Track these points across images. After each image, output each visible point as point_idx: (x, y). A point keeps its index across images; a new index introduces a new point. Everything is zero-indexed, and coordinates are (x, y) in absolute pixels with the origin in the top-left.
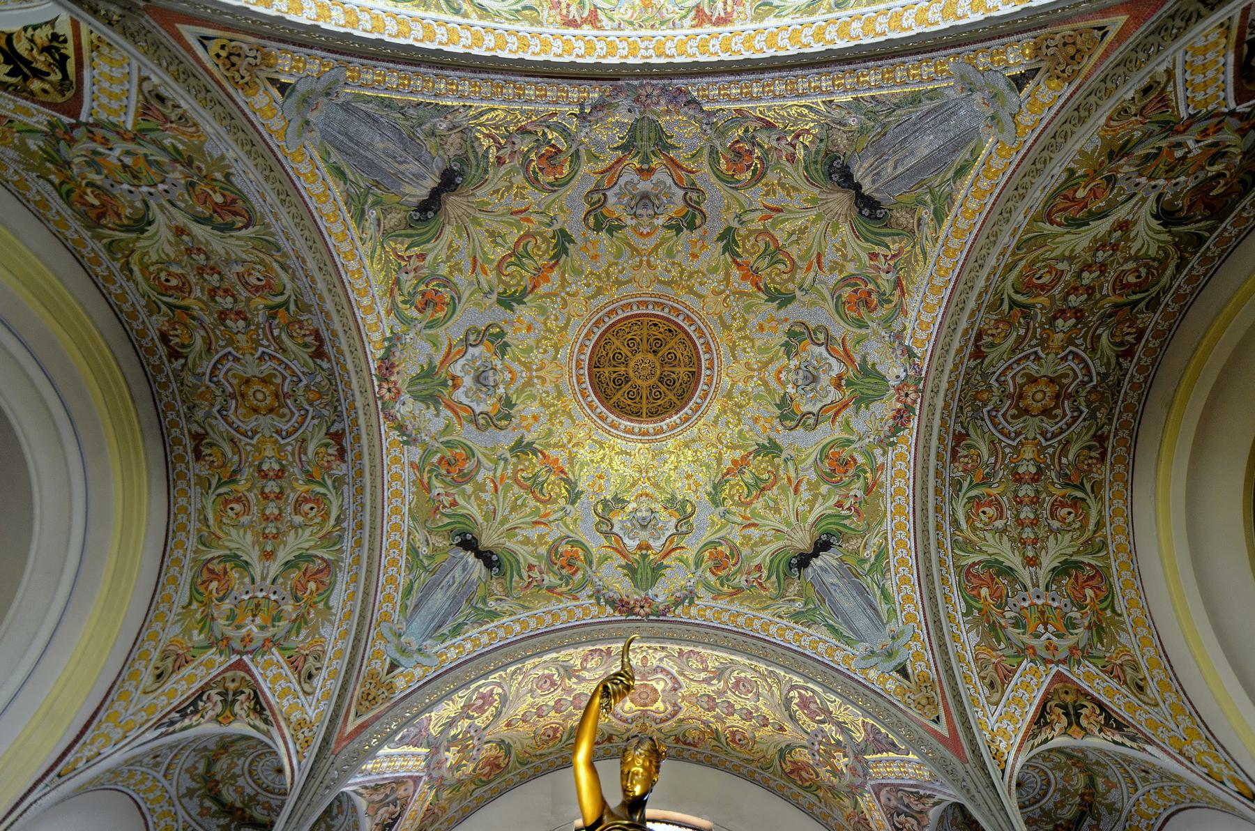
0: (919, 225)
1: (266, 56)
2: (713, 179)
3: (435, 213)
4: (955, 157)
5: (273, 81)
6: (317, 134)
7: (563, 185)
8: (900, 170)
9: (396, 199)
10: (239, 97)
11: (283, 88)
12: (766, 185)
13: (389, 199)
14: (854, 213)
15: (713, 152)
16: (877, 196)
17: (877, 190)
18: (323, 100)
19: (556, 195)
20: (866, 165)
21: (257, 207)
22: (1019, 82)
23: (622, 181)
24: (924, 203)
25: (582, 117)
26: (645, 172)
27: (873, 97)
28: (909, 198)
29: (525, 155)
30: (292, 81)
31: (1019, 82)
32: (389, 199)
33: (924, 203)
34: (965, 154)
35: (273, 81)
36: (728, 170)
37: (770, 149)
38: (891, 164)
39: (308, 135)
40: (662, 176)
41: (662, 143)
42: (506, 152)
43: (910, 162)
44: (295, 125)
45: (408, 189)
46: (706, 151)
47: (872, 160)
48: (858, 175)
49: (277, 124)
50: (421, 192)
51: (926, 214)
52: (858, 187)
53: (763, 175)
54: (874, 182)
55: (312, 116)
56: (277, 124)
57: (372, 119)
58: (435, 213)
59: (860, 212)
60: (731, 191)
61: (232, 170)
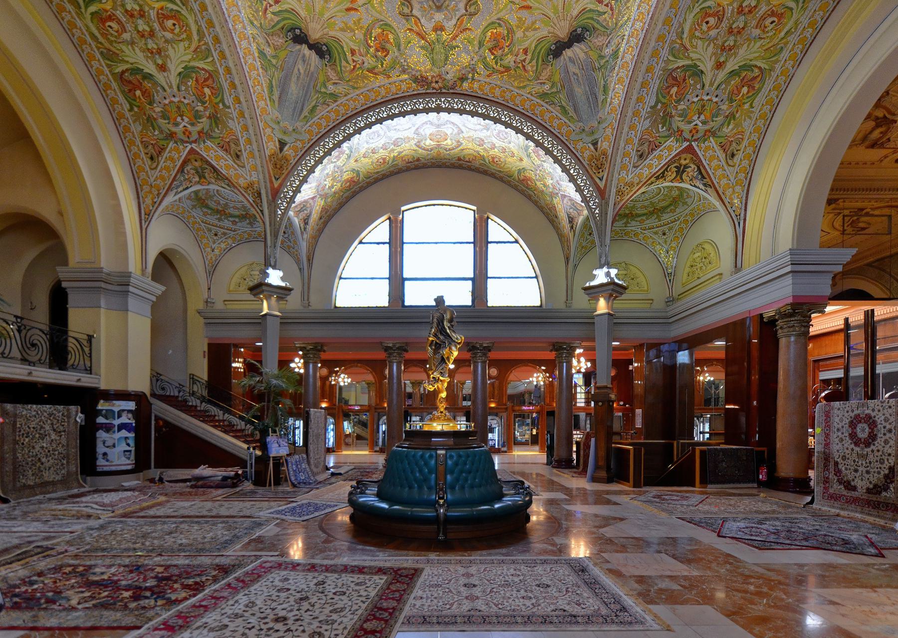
0: (267, 42)
1: (590, 160)
2: (394, 25)
3: (576, 30)
4: (280, 91)
5: (596, 149)
6: (600, 115)
7: (493, 23)
8: (296, 70)
9: (591, 53)
10: (610, 152)
11: (595, 144)
12: (361, 28)
13: (594, 55)
14: (303, 26)
15: (398, 46)
16: (298, 47)
17: (300, 51)
18: (587, 129)
19: (499, 16)
20: (313, 64)
21: (658, 82)
22: (282, 144)
23: (454, 22)
24: (274, 57)
25: (474, 70)
26: (439, 28)
27: (329, 105)
28: (282, 55)
29: (511, 52)
30: (590, 145)
31: (282, 144)
32: (594, 55)
33: (274, 57)
34: (276, 97)
35: (596, 149)
36: (387, 35)
37: (366, 55)
38: (302, 71)
39: (603, 117)
40: (428, 26)
41: (430, 48)
42: (522, 57)
43: (294, 79)
44: (604, 125)
45: (582, 55)
46: (402, 48)
47: (312, 68)
48: (313, 53)
49: (609, 131)
50: (577, 50)
51: (269, 51)
52: (311, 47)
53: (365, 35)
54: (304, 56)
55: (595, 124)
56: (609, 131)
57: (576, 110)
58: (576, 30)
59: (300, 30)
60: (383, 18)
61: (649, 109)
